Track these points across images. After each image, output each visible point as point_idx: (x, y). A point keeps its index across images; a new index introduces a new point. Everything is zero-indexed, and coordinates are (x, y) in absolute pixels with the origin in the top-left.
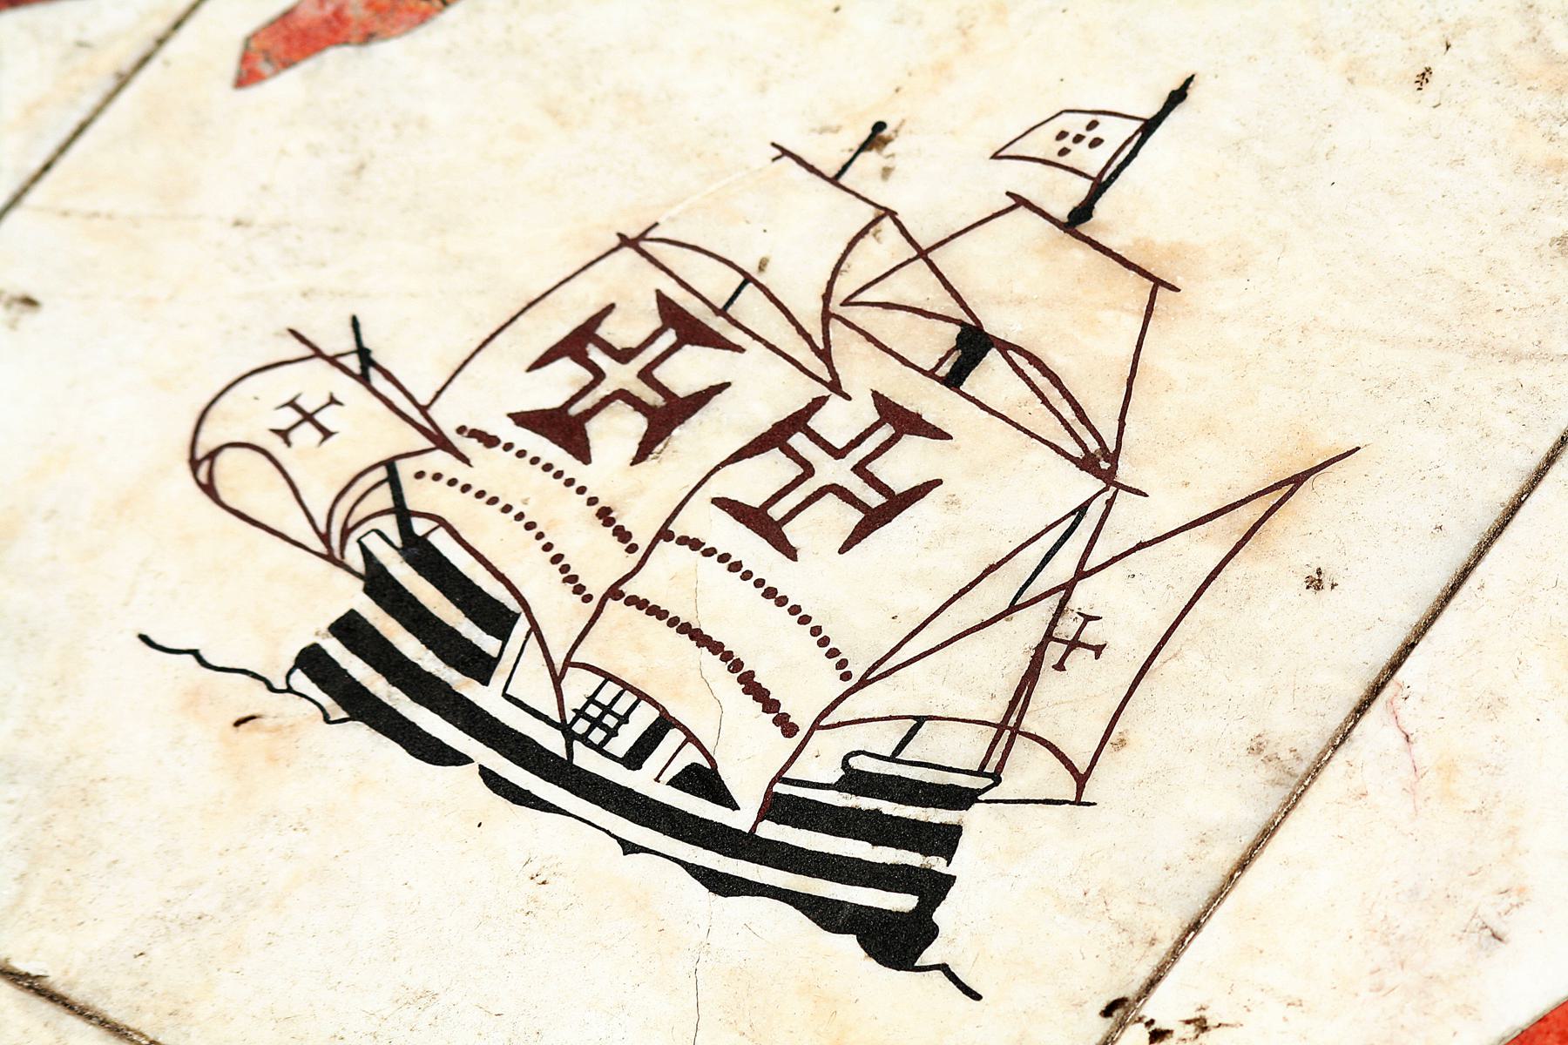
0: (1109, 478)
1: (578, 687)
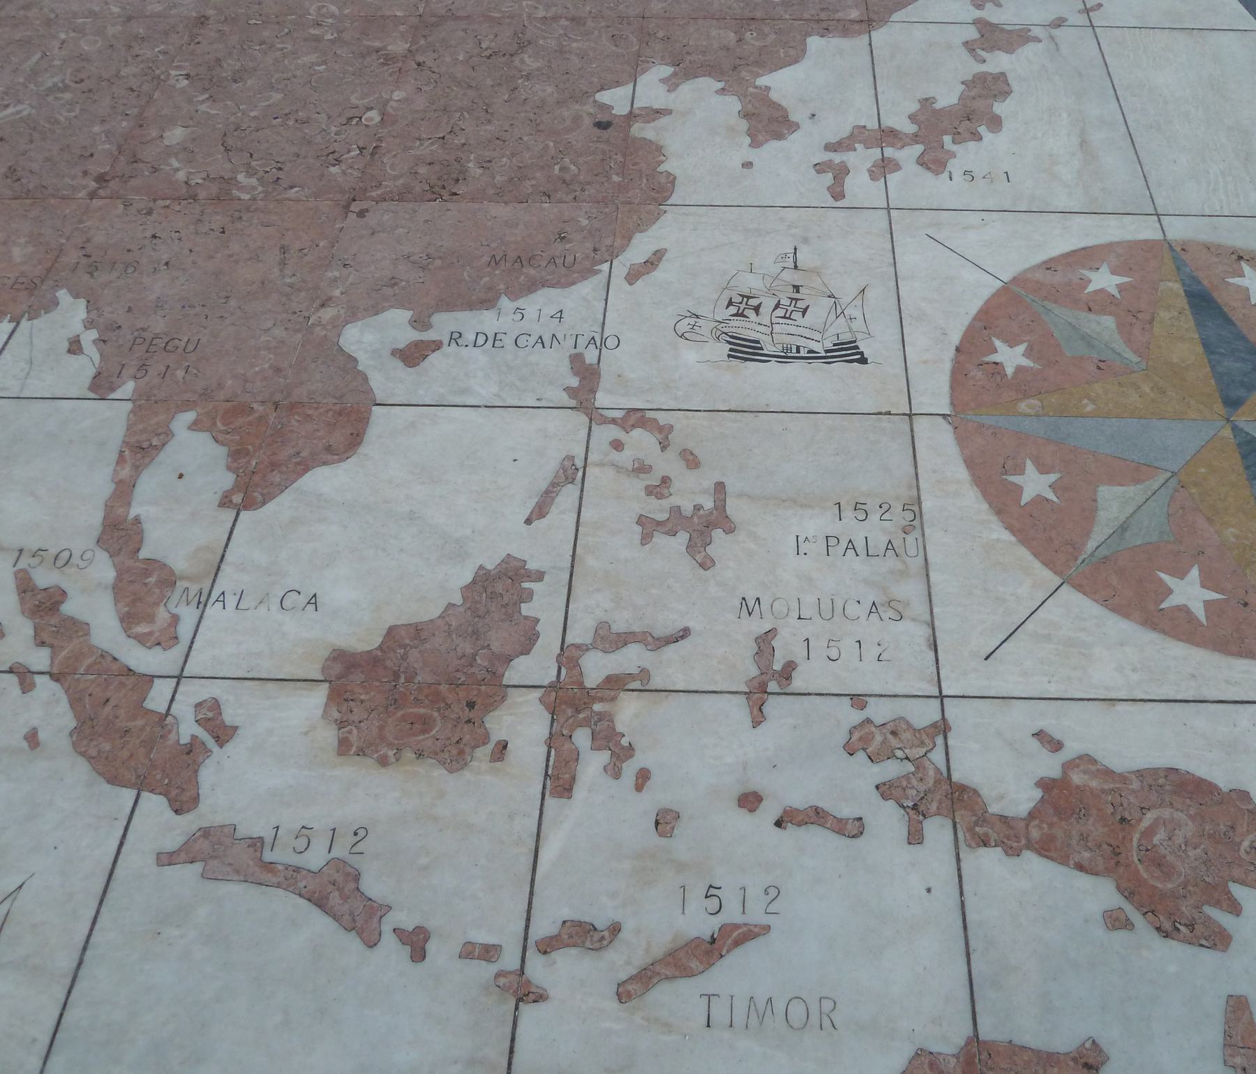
0: (834, 297)
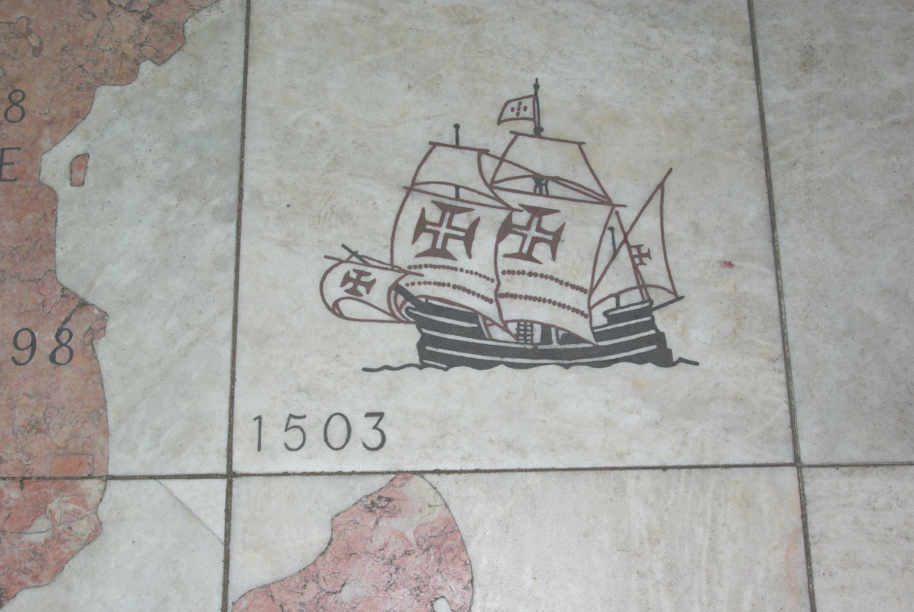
1: (512, 327)
